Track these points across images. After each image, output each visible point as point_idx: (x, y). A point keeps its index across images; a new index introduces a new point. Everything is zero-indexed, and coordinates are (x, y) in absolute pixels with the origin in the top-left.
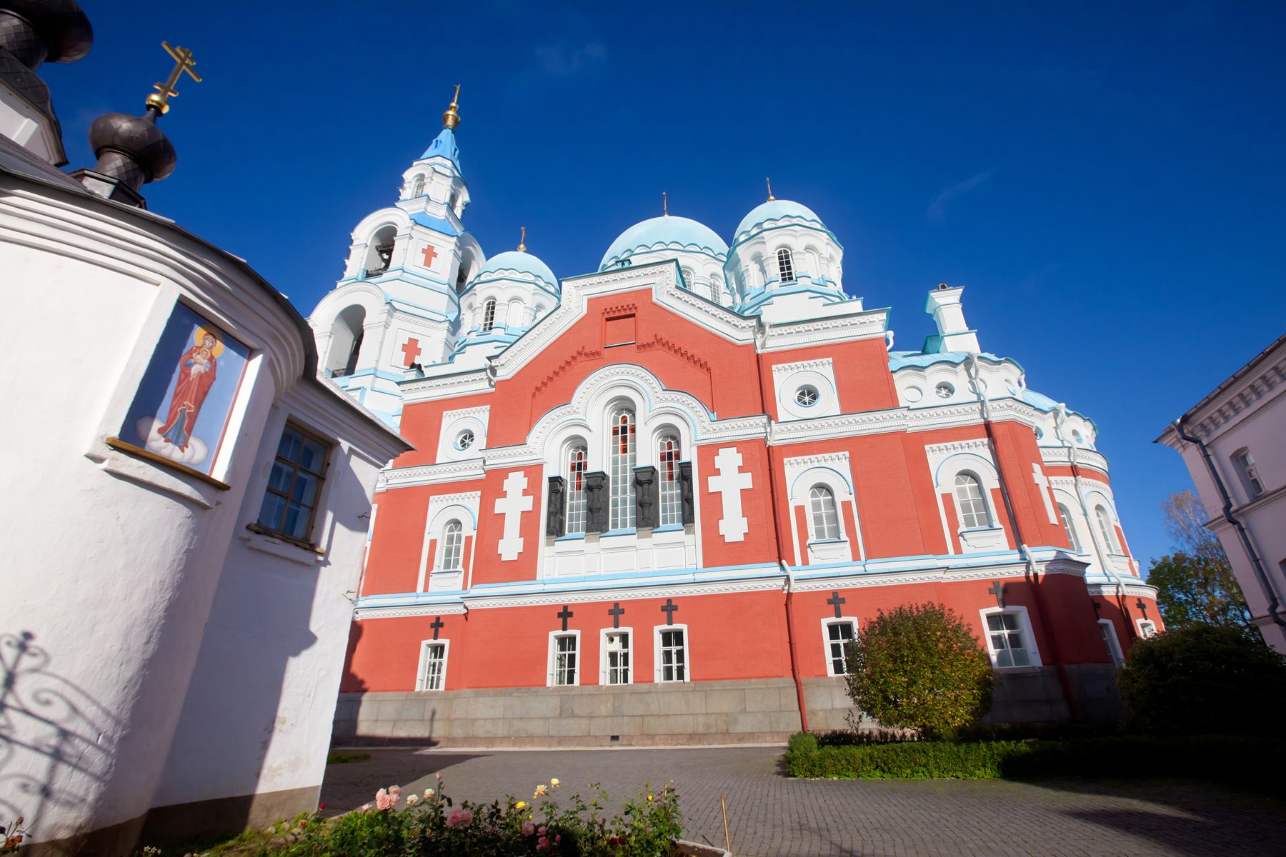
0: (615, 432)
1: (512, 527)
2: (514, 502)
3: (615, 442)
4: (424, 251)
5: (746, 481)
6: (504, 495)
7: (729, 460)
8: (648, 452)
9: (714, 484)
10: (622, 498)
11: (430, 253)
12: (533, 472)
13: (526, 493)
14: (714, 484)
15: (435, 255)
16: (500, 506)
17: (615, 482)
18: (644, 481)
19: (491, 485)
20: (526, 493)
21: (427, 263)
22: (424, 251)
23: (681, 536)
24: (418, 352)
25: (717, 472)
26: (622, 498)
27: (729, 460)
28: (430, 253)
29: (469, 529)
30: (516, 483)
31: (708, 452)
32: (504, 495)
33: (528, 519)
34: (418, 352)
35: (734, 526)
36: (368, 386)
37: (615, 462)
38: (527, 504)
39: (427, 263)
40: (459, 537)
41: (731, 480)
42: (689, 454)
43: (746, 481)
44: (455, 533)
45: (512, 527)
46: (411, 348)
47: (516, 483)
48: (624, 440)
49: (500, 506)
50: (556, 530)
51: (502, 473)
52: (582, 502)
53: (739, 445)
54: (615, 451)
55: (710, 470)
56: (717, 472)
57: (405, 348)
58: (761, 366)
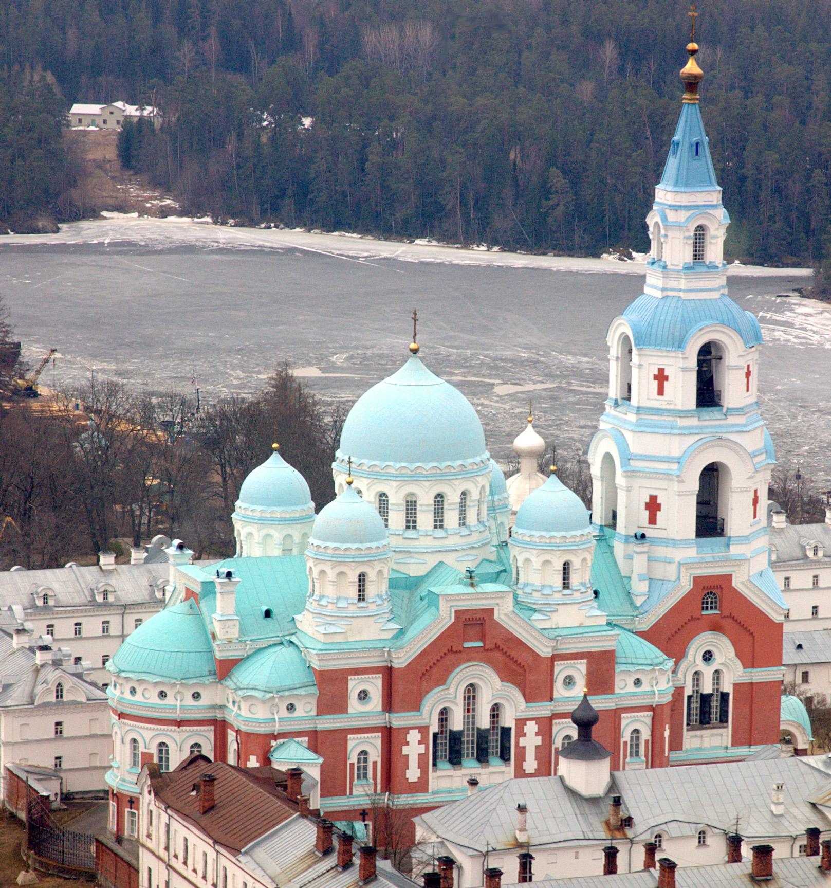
6: (407, 744)
7: (531, 728)
9: (523, 742)
12: (423, 730)
13: (420, 743)
14: (523, 742)
20: (420, 743)
23: (503, 768)
27: (531, 728)
31: (521, 723)
32: (407, 744)
33: (422, 758)
35: (530, 765)
38: (422, 749)
53: (537, 720)
55: (521, 733)
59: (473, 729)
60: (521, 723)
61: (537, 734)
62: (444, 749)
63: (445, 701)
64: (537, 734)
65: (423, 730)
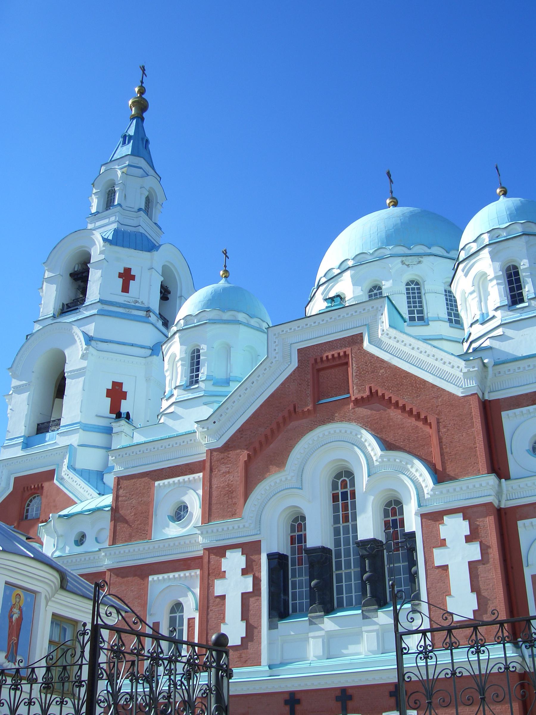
0: (335, 498)
1: (233, 608)
2: (234, 582)
3: (336, 509)
4: (120, 275)
5: (474, 552)
6: (222, 575)
8: (368, 526)
9: (440, 557)
10: (348, 575)
11: (127, 276)
14: (440, 557)
15: (133, 278)
16: (219, 587)
17: (338, 555)
18: (371, 550)
19: (208, 564)
20: (244, 572)
21: (125, 289)
22: (120, 275)
24: (124, 395)
25: (443, 543)
26: (348, 575)
27: (455, 528)
28: (127, 276)
29: (191, 610)
30: (234, 561)
32: (222, 575)
34: (124, 395)
35: (462, 604)
36: (75, 444)
37: (337, 532)
39: (125, 289)
40: (181, 618)
41: (457, 551)
42: (412, 523)
43: (474, 552)
44: (178, 615)
45: (233, 608)
46: (116, 393)
47: (234, 561)
48: (345, 507)
49: (219, 587)
50: (280, 610)
51: (220, 551)
52: (302, 581)
53: (466, 512)
54: (336, 520)
56: (443, 543)
57: (109, 393)
58: (490, 412)
59: (347, 542)
60: (432, 518)
61: (469, 539)
62: (300, 581)
63: (292, 496)
64: (469, 539)
65: (251, 549)
